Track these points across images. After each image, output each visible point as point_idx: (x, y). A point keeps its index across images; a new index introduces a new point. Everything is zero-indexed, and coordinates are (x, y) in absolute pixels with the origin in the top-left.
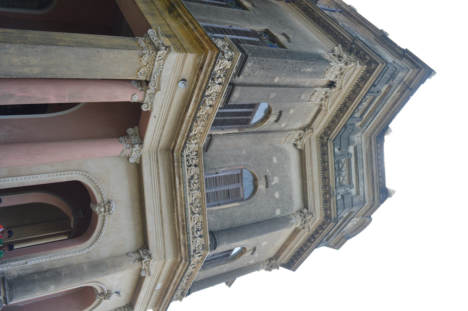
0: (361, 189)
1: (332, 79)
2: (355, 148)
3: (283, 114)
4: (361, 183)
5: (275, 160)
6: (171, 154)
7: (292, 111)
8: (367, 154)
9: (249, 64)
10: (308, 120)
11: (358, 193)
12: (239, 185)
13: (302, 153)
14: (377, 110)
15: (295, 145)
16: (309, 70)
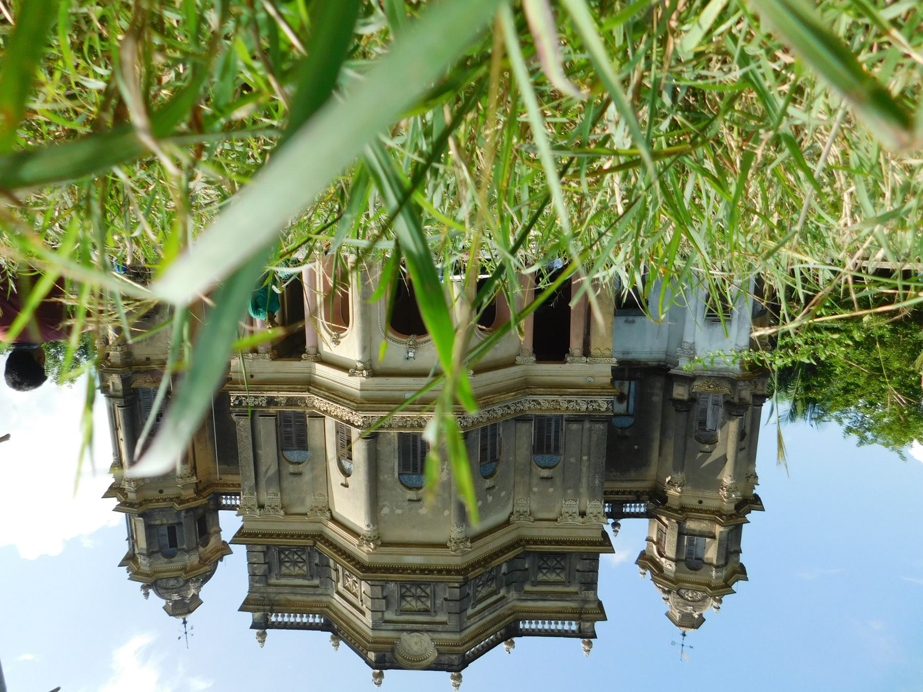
0: (472, 620)
1: (588, 511)
2: (503, 597)
3: (549, 483)
4: (477, 618)
5: (503, 494)
6: (526, 386)
7: (551, 490)
8: (499, 616)
9: (601, 426)
10: (540, 516)
11: (469, 618)
12: (489, 460)
13: (507, 523)
14: (549, 597)
15: (512, 513)
16: (597, 482)
